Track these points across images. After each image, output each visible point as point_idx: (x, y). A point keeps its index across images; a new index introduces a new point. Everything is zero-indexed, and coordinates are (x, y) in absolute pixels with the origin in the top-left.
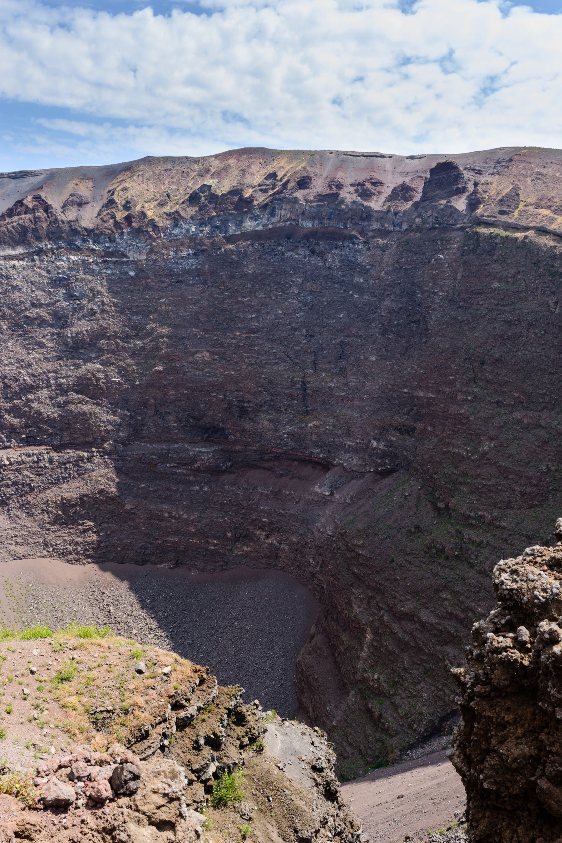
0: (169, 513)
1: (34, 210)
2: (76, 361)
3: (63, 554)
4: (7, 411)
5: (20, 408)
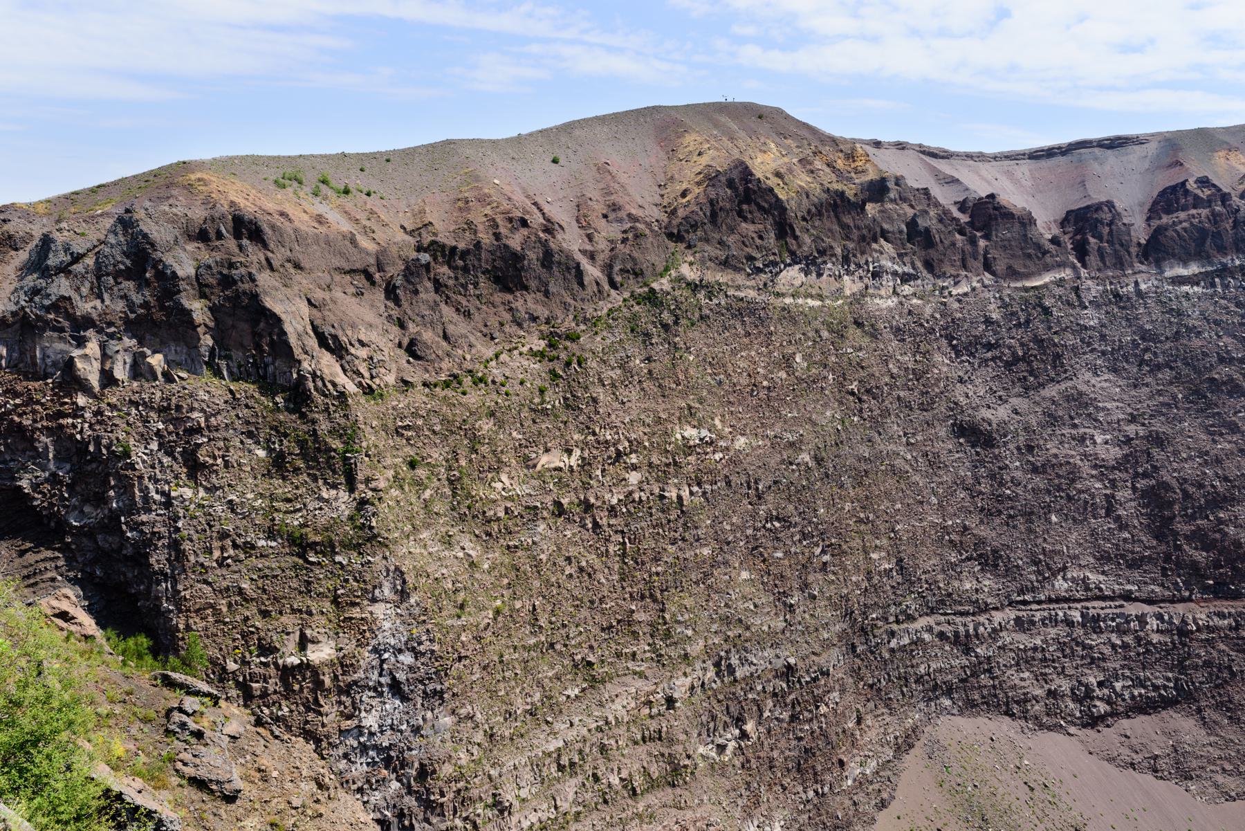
1: (1209, 202)
4: (1186, 537)
5: (1206, 534)
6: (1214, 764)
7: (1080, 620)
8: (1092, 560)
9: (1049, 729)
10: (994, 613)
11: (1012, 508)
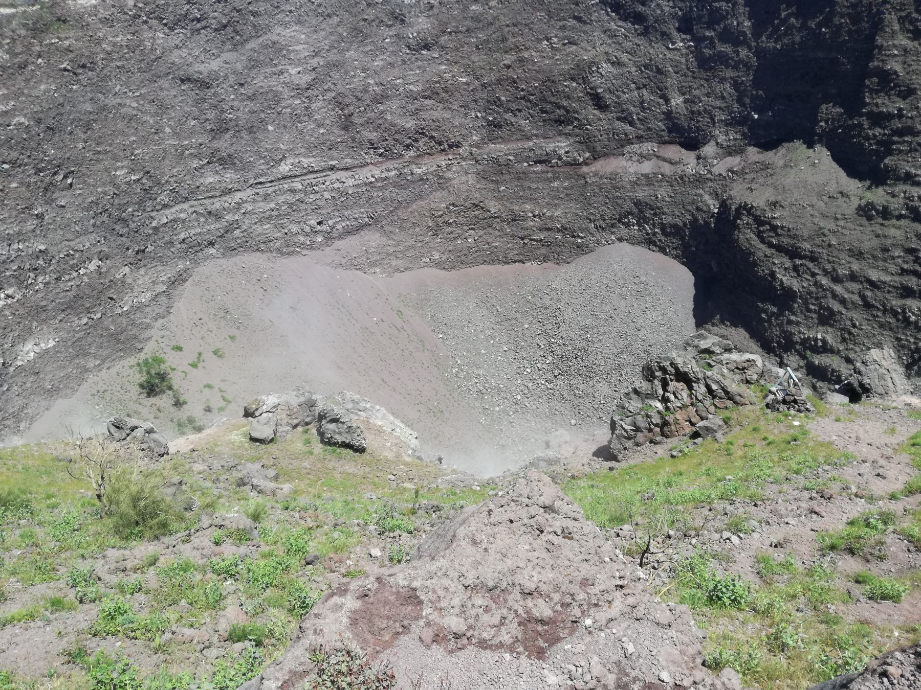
0: (532, 213)
2: (420, 63)
3: (439, 265)
6: (391, 255)
7: (300, 187)
8: (304, 150)
9: (288, 254)
10: (236, 193)
11: (237, 126)
